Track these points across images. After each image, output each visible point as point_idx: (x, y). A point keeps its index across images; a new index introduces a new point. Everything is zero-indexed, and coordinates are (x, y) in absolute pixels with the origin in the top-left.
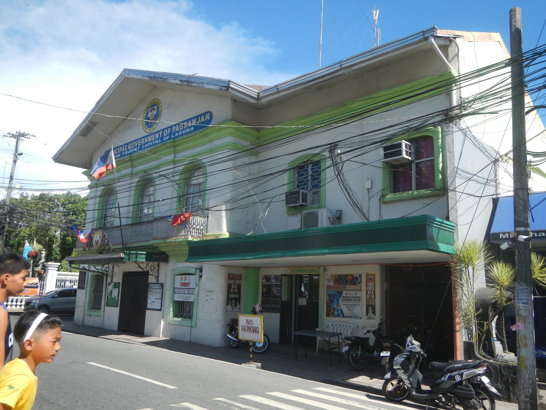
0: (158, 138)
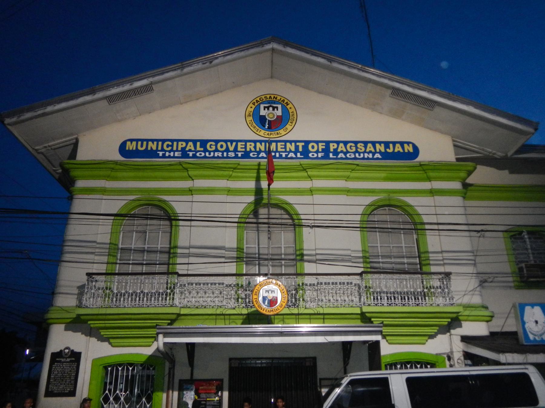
0: (293, 149)
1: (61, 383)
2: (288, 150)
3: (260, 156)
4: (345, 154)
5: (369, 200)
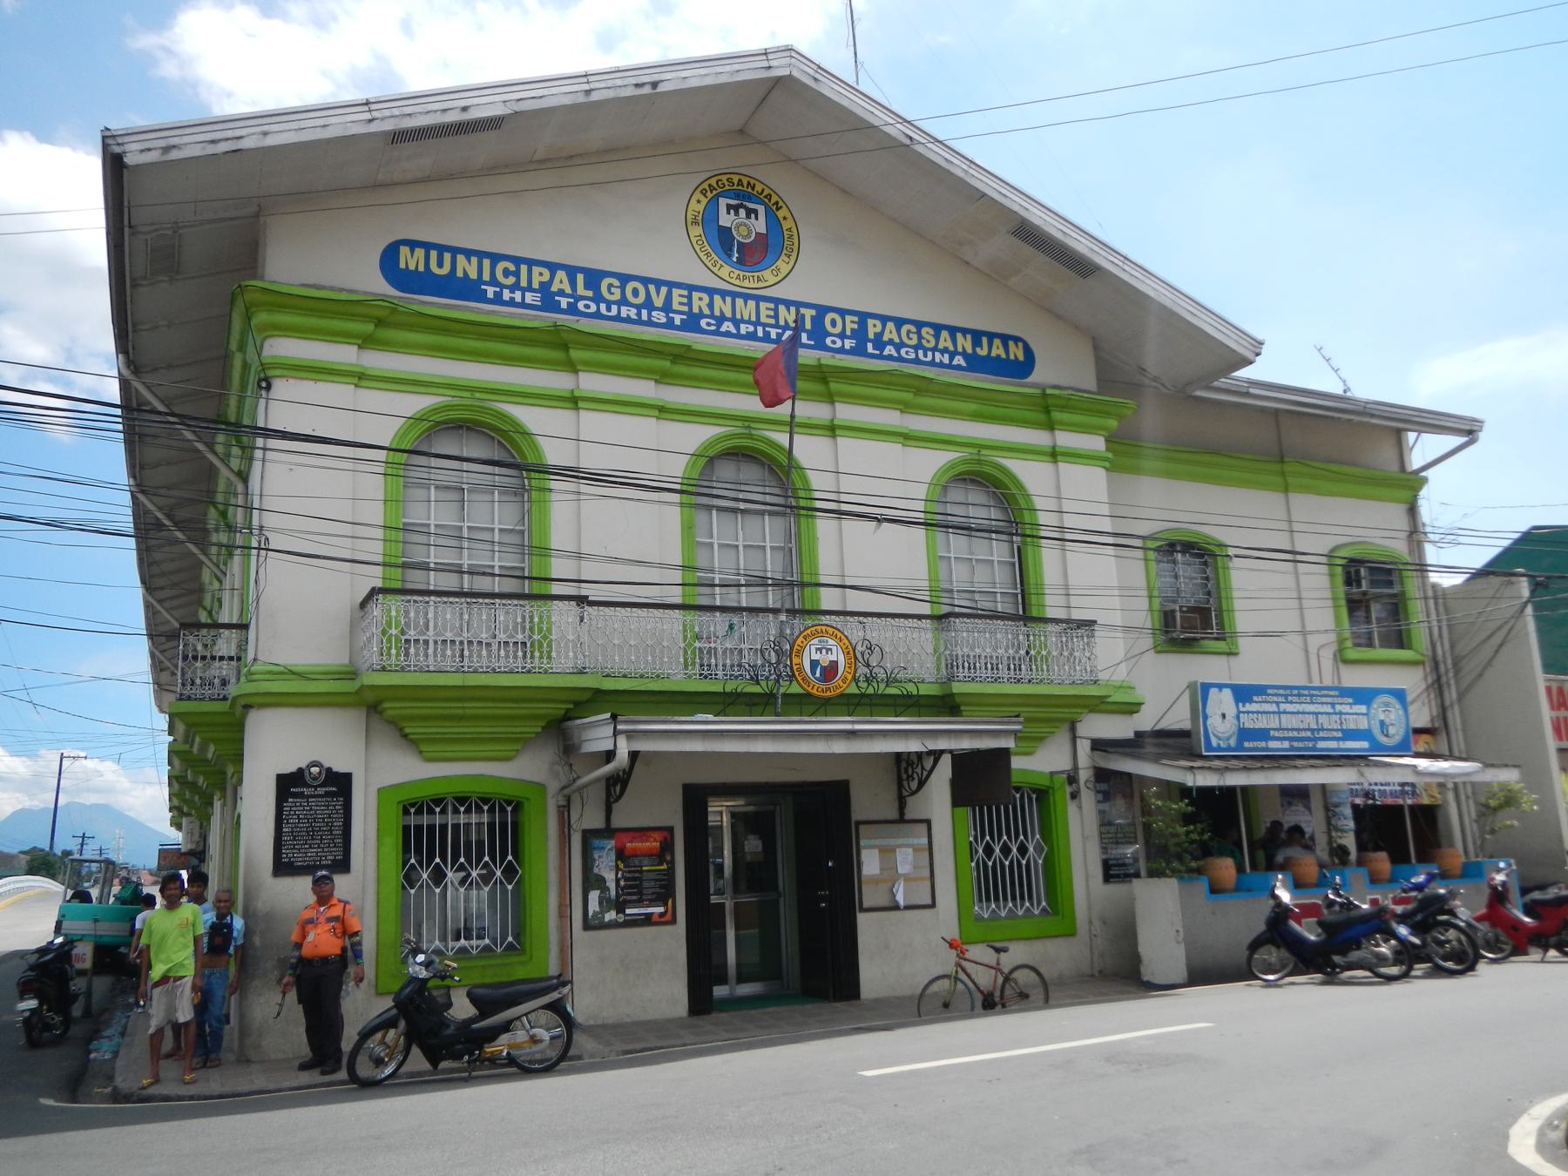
1: (310, 845)
2: (782, 323)
3: (723, 329)
4: (898, 347)
5: (942, 458)
